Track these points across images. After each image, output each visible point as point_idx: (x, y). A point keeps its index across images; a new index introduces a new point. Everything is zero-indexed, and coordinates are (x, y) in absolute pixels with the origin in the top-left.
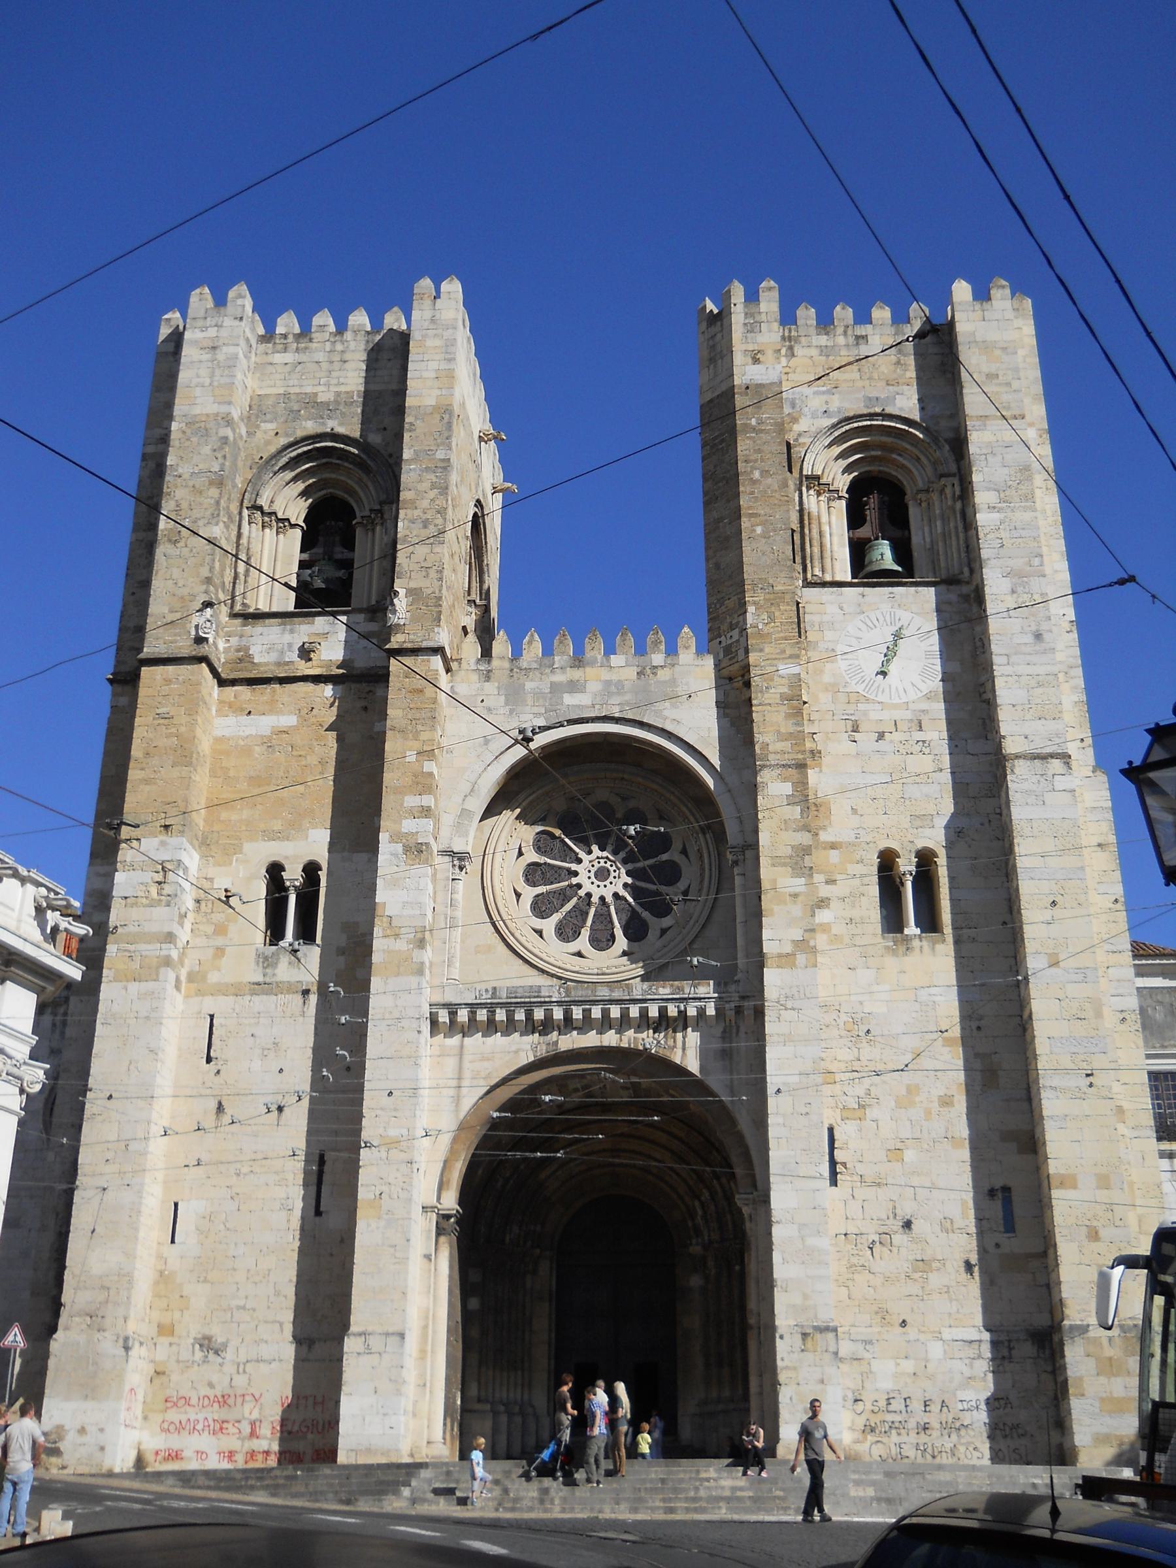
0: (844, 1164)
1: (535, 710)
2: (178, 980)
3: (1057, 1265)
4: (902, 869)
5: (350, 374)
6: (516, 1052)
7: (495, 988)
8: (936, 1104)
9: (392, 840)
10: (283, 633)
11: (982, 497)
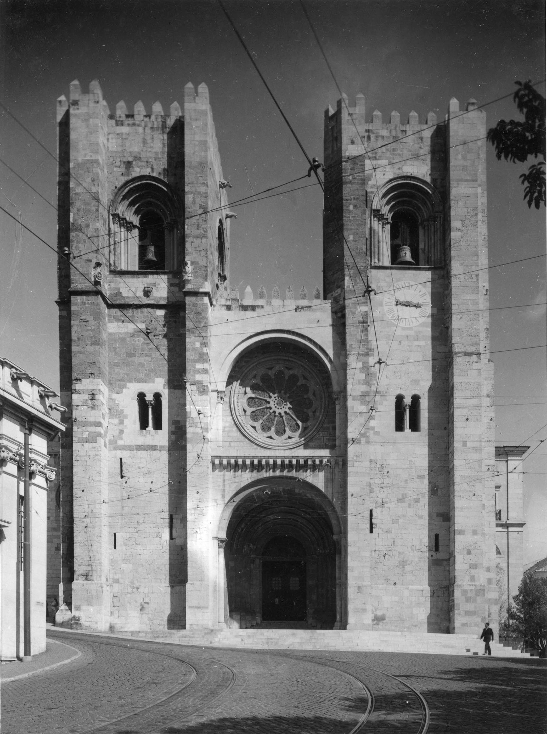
0: (376, 524)
2: (105, 442)
3: (455, 563)
4: (405, 403)
8: (413, 502)
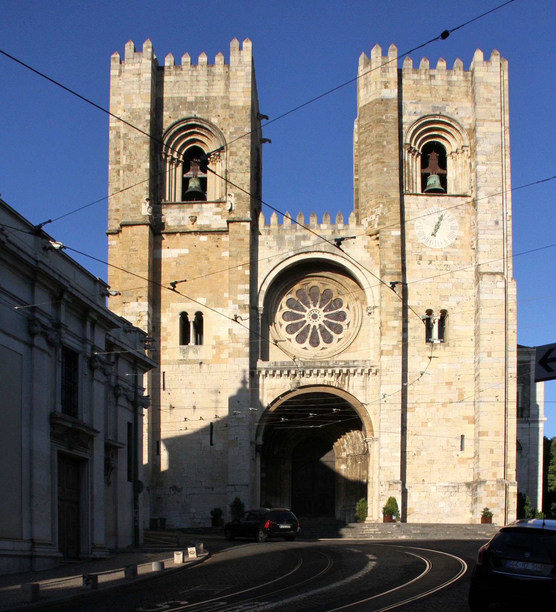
1: (289, 247)
5: (201, 88)
6: (284, 386)
7: (276, 362)
9: (233, 303)
10: (180, 211)
11: (481, 158)
